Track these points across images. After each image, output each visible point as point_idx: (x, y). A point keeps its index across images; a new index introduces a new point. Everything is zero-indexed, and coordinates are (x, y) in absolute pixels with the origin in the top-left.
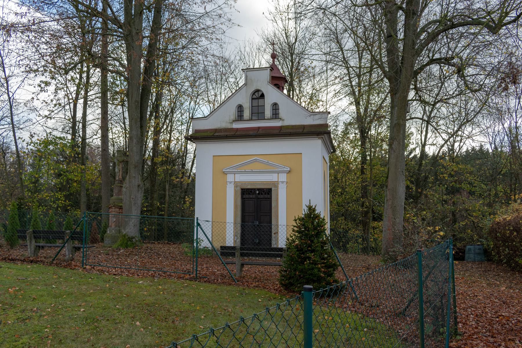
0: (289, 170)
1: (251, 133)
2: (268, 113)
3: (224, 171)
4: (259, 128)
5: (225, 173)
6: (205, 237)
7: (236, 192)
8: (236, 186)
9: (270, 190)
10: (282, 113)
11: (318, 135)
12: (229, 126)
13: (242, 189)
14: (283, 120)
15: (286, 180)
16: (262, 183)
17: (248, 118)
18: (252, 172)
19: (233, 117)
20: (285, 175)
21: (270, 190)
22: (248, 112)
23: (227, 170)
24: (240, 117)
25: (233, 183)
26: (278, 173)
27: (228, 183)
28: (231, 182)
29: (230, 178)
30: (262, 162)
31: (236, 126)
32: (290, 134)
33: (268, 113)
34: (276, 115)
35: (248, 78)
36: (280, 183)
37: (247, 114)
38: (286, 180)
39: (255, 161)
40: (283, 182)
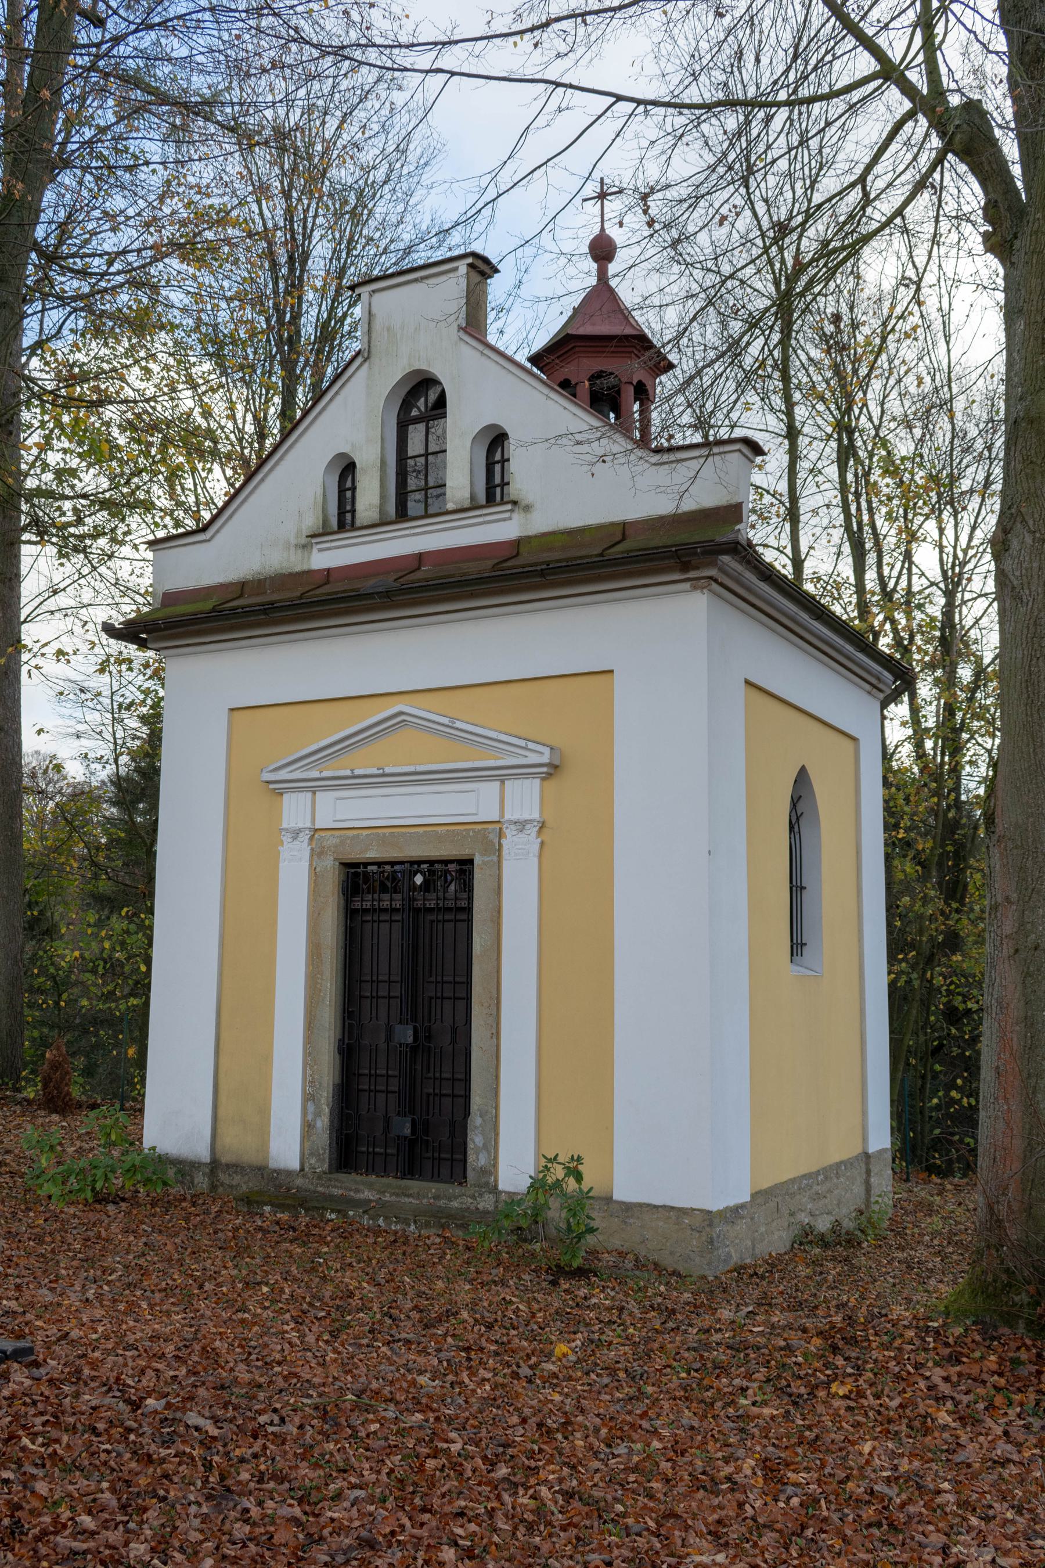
0: (545, 759)
1: (368, 585)
2: (460, 475)
3: (267, 776)
4: (420, 558)
5: (277, 790)
6: (176, 1114)
7: (316, 878)
8: (317, 853)
9: (465, 867)
10: (523, 471)
11: (685, 567)
12: (296, 562)
13: (346, 865)
14: (527, 508)
15: (536, 815)
16: (430, 830)
17: (373, 515)
18: (383, 779)
19: (311, 521)
20: (533, 786)
21: (465, 867)
22: (376, 484)
23: (283, 775)
24: (344, 519)
25: (305, 837)
26: (501, 775)
27: (287, 838)
28: (296, 833)
29: (295, 811)
30: (428, 728)
31: (329, 557)
32: (542, 573)
33: (460, 475)
34: (494, 491)
35: (377, 324)
36: (510, 832)
37: (369, 497)
38: (536, 815)
39: (397, 722)
40: (521, 825)
